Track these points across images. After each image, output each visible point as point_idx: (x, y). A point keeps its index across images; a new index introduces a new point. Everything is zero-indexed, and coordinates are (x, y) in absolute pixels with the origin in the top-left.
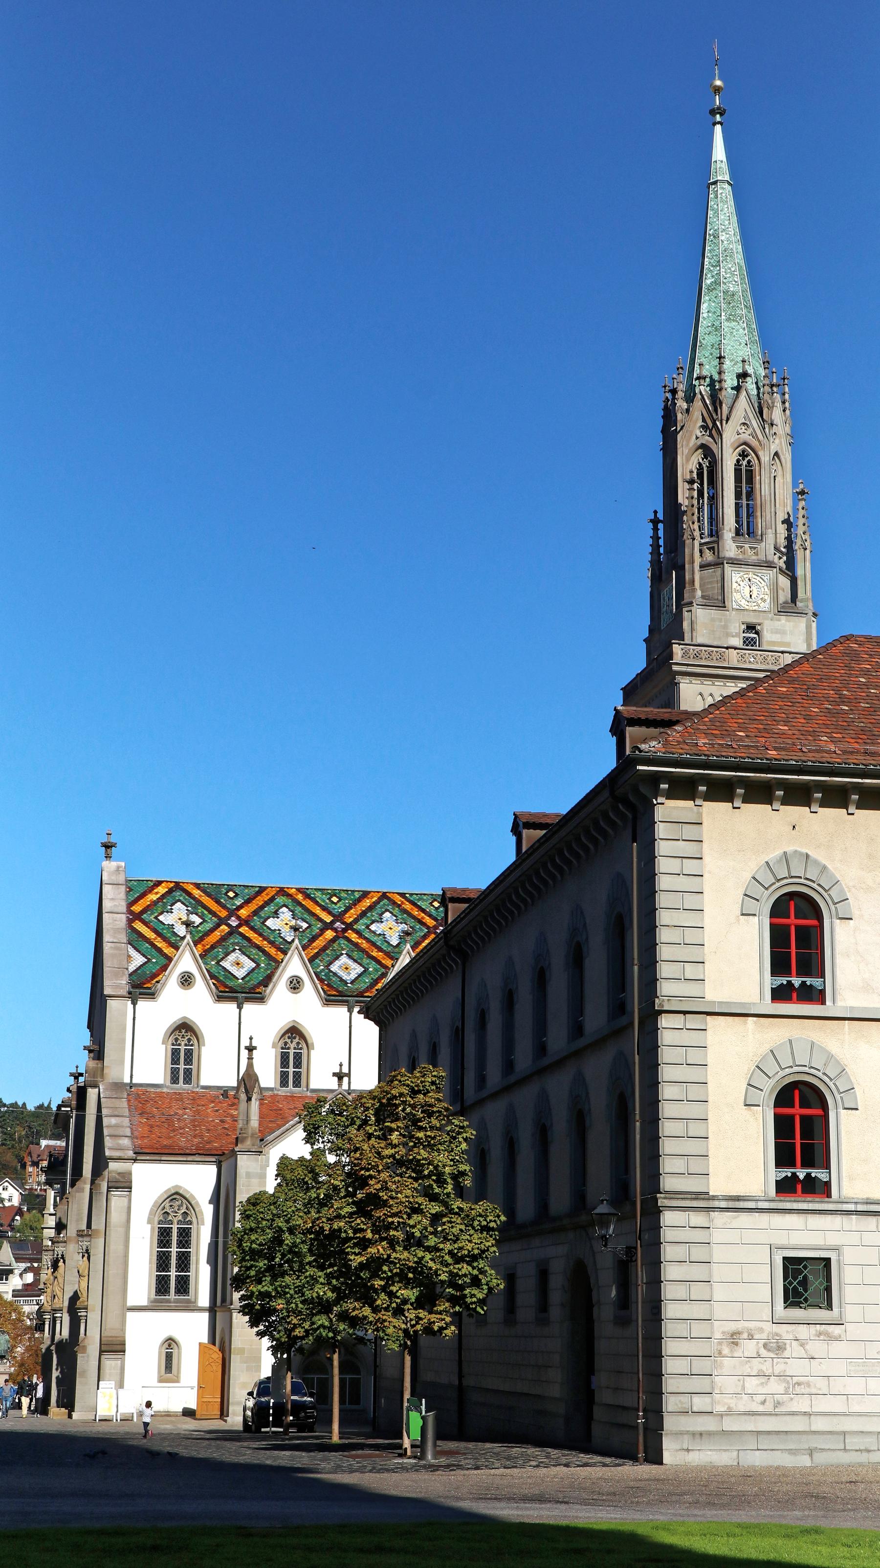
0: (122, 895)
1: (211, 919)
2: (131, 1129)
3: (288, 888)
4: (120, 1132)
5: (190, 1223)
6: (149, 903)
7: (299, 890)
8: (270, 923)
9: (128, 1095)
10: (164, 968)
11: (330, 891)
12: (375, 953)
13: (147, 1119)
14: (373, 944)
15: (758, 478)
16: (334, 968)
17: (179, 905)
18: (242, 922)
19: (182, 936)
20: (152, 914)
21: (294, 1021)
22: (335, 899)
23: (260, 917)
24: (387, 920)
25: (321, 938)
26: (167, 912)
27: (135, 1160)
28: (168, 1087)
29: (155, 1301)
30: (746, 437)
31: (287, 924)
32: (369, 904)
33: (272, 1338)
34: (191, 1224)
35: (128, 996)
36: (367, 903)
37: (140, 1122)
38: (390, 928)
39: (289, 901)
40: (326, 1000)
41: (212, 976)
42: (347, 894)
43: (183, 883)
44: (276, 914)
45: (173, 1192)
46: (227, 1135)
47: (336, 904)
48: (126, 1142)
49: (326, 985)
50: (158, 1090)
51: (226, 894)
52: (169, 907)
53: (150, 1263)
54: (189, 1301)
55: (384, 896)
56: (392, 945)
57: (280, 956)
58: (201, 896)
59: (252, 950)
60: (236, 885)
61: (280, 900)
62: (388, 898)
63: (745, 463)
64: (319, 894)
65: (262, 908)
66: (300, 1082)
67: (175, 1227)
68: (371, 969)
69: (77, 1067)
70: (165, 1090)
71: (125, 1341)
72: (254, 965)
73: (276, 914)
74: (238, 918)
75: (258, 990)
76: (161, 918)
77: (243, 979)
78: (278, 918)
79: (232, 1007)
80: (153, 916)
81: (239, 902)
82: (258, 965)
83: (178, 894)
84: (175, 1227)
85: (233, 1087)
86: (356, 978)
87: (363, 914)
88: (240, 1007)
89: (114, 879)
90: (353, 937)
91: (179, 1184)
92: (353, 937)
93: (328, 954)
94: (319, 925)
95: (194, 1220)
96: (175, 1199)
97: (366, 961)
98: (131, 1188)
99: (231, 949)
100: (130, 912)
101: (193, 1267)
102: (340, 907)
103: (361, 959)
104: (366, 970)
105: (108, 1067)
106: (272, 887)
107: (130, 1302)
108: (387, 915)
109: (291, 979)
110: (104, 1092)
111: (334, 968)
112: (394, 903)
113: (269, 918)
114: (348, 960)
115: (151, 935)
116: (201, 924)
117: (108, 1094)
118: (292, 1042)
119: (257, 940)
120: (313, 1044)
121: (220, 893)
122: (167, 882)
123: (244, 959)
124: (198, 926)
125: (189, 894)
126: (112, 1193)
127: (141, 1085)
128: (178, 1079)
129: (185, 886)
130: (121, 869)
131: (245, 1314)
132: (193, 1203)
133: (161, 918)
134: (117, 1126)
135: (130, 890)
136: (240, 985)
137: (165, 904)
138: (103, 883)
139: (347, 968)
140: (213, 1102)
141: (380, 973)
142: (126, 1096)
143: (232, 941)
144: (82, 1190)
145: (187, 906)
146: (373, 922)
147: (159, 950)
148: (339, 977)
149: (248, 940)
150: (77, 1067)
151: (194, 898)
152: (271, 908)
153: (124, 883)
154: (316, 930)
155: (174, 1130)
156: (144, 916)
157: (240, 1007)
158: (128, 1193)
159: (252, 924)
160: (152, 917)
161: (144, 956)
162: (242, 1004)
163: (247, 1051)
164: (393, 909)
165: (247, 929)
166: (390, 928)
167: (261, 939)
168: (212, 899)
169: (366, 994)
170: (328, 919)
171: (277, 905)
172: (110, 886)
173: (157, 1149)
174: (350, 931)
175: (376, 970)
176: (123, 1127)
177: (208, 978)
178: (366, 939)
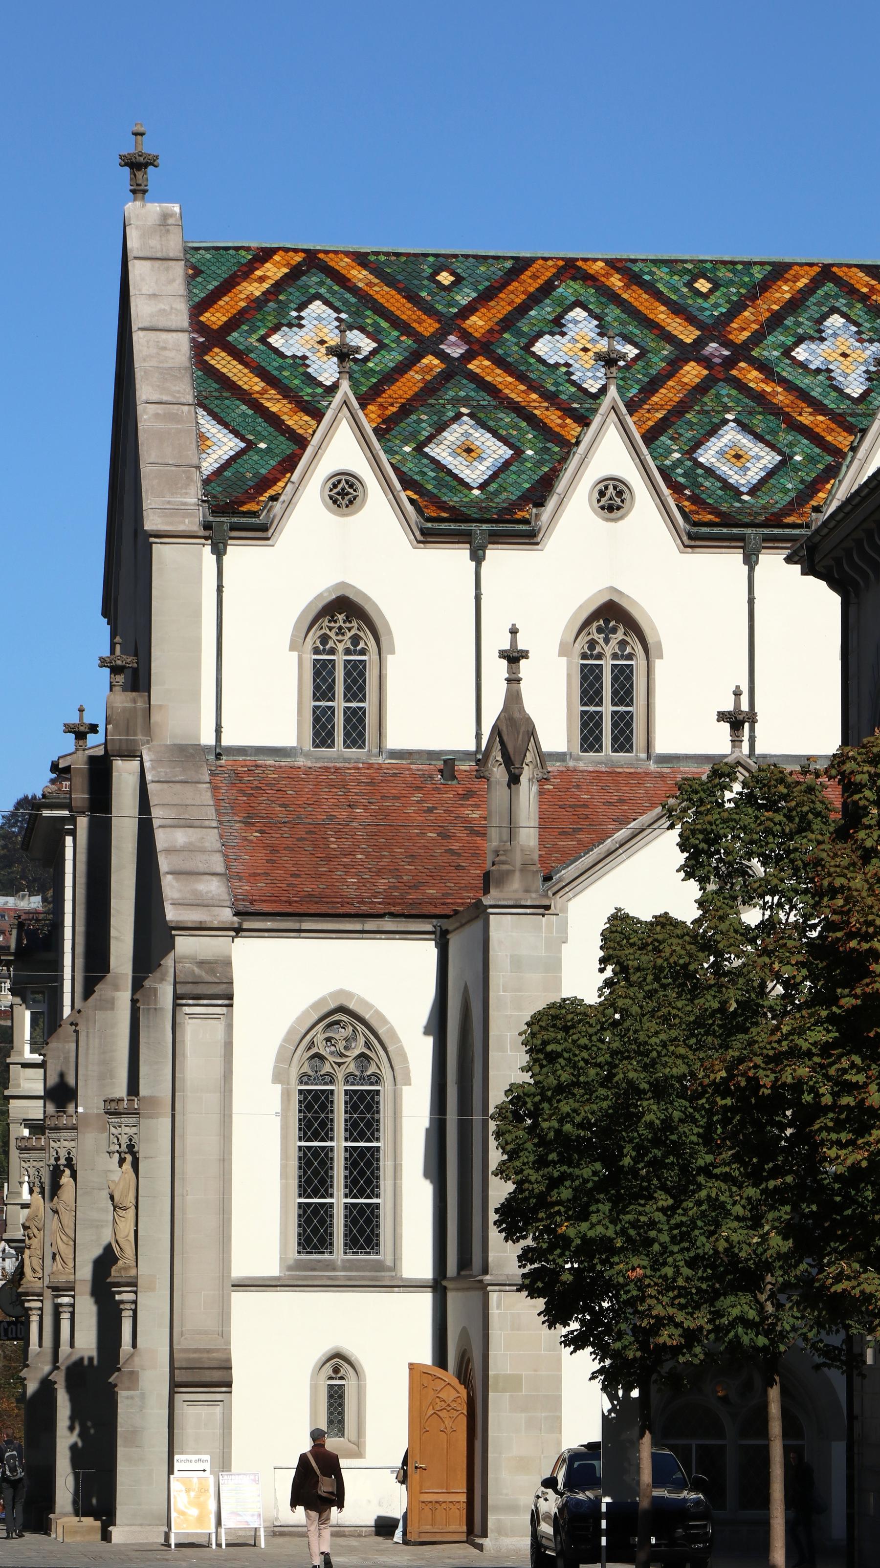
0: (178, 286)
1: (397, 340)
2: (226, 856)
3: (585, 260)
4: (199, 863)
5: (376, 1079)
6: (243, 304)
7: (613, 264)
8: (542, 347)
9: (213, 774)
10: (289, 464)
11: (689, 266)
12: (806, 419)
13: (262, 832)
14: (803, 395)
16: (707, 456)
17: (317, 307)
18: (476, 347)
19: (328, 383)
20: (252, 331)
21: (613, 589)
22: (703, 285)
23: (519, 334)
24: (835, 335)
25: (671, 383)
26: (290, 325)
27: (238, 931)
28: (307, 755)
29: (298, 1266)
31: (585, 350)
32: (788, 296)
33: (602, 1351)
34: (377, 1083)
35: (202, 533)
36: (785, 291)
37: (245, 839)
38: (844, 355)
39: (589, 294)
40: (690, 536)
41: (407, 483)
42: (734, 271)
43: (326, 252)
44: (557, 326)
45: (332, 1005)
46: (458, 867)
47: (705, 296)
48: (214, 888)
49: (689, 498)
50: (285, 762)
51: (432, 277)
52: (294, 314)
53: (284, 1175)
54: (379, 1266)
55: (826, 273)
56: (848, 397)
57: (572, 429)
58: (370, 284)
59: (501, 415)
60: (455, 256)
61: (567, 290)
62: (837, 281)
64: (662, 273)
65: (522, 310)
66: (629, 739)
67: (340, 1090)
68: (798, 458)
70: (301, 762)
71: (229, 1360)
72: (508, 453)
73: (557, 326)
74: (465, 336)
75: (520, 515)
76: (275, 340)
77: (482, 487)
78: (563, 334)
79: (460, 555)
80: (255, 337)
81: (464, 297)
82: (518, 453)
83: (312, 280)
84: (340, 1090)
85: (467, 754)
86: (763, 481)
87: (775, 321)
88: (478, 557)
89: (155, 245)
90: (753, 377)
91: (347, 988)
92: (753, 377)
93: (690, 424)
94: (666, 350)
95: (386, 1073)
96: (337, 1023)
97: (785, 438)
98: (230, 997)
99: (451, 414)
100: (198, 326)
101: (386, 1184)
102: (716, 306)
103: (774, 432)
104: (786, 460)
105: (160, 707)
106: (545, 259)
107: (239, 1270)
108: (836, 321)
109: (601, 486)
110: (153, 768)
111: (707, 456)
112: (851, 291)
113: (540, 335)
114: (739, 437)
115: (253, 384)
116: (374, 353)
117: (164, 772)
118: (607, 641)
119: (515, 390)
120: (659, 644)
121: (418, 275)
122: (287, 250)
123: (483, 439)
124: (366, 359)
125: (342, 280)
126: (187, 1010)
127: (242, 751)
128: (331, 734)
129: (332, 261)
130: (171, 221)
131: (533, 1293)
132: (381, 1032)
133: (275, 340)
134: (190, 850)
135: (195, 273)
136: (475, 503)
137: (283, 308)
138: (130, 255)
139: (738, 457)
140: (419, 788)
141: (821, 466)
142: (207, 778)
143: (451, 393)
144: (110, 1005)
145: (337, 310)
146: (800, 340)
147: (274, 420)
148: (719, 478)
149: (492, 390)
150: (81, 710)
151: (354, 290)
152: (546, 311)
153: (182, 255)
154: (659, 364)
155: (328, 859)
156: (234, 337)
157: (478, 557)
158: (224, 1010)
159: (500, 352)
160: (253, 340)
161: (236, 434)
162: (483, 548)
163: (504, 663)
164: (850, 306)
165: (487, 363)
166: (844, 355)
167: (523, 388)
168: (399, 291)
169: (790, 520)
170: (688, 335)
171: (560, 302)
172: (147, 264)
173: (290, 903)
174: (742, 364)
175: (810, 459)
176: (203, 851)
177: (398, 486)
178: (783, 382)
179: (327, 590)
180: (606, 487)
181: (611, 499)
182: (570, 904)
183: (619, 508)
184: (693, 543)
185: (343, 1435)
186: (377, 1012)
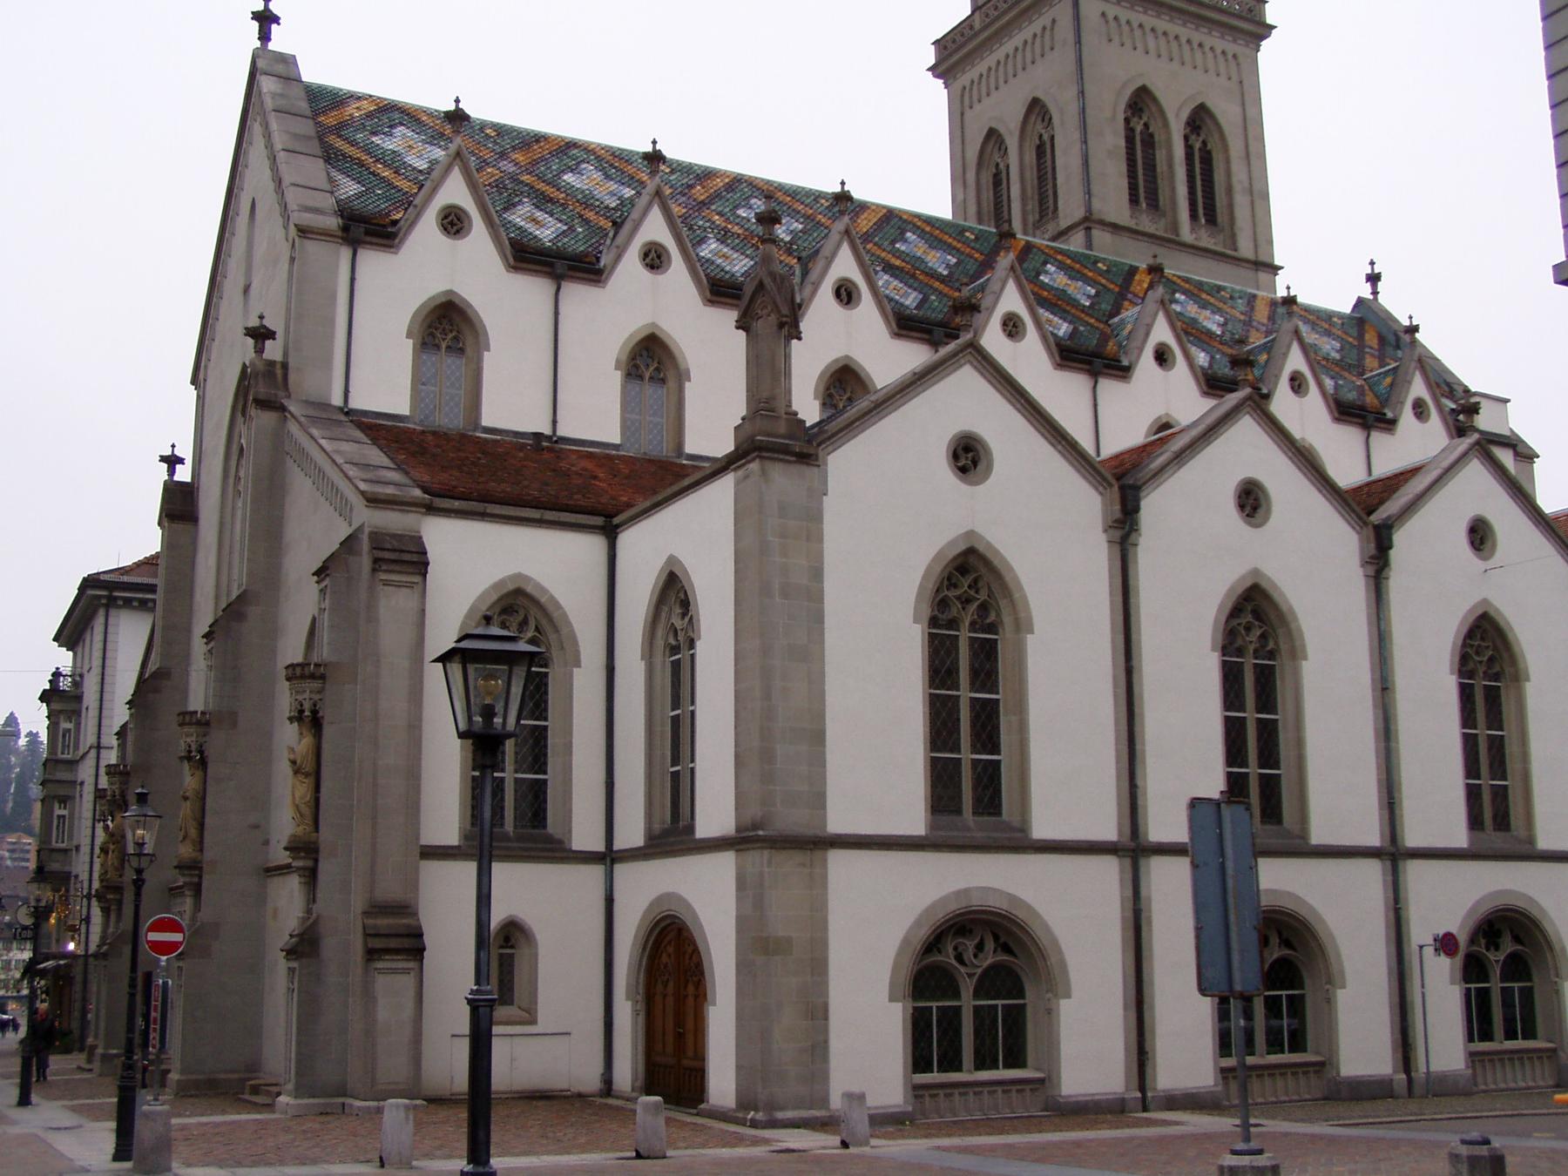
27: (431, 510)
35: (340, 233)
54: (550, 839)
69: (173, 446)
71: (421, 927)
85: (549, 438)
120: (688, 372)
127: (365, 413)
133: (376, 139)
150: (173, 446)
180: (650, 251)
181: (653, 259)
182: (829, 457)
184: (714, 298)
185: (511, 1003)
186: (552, 598)
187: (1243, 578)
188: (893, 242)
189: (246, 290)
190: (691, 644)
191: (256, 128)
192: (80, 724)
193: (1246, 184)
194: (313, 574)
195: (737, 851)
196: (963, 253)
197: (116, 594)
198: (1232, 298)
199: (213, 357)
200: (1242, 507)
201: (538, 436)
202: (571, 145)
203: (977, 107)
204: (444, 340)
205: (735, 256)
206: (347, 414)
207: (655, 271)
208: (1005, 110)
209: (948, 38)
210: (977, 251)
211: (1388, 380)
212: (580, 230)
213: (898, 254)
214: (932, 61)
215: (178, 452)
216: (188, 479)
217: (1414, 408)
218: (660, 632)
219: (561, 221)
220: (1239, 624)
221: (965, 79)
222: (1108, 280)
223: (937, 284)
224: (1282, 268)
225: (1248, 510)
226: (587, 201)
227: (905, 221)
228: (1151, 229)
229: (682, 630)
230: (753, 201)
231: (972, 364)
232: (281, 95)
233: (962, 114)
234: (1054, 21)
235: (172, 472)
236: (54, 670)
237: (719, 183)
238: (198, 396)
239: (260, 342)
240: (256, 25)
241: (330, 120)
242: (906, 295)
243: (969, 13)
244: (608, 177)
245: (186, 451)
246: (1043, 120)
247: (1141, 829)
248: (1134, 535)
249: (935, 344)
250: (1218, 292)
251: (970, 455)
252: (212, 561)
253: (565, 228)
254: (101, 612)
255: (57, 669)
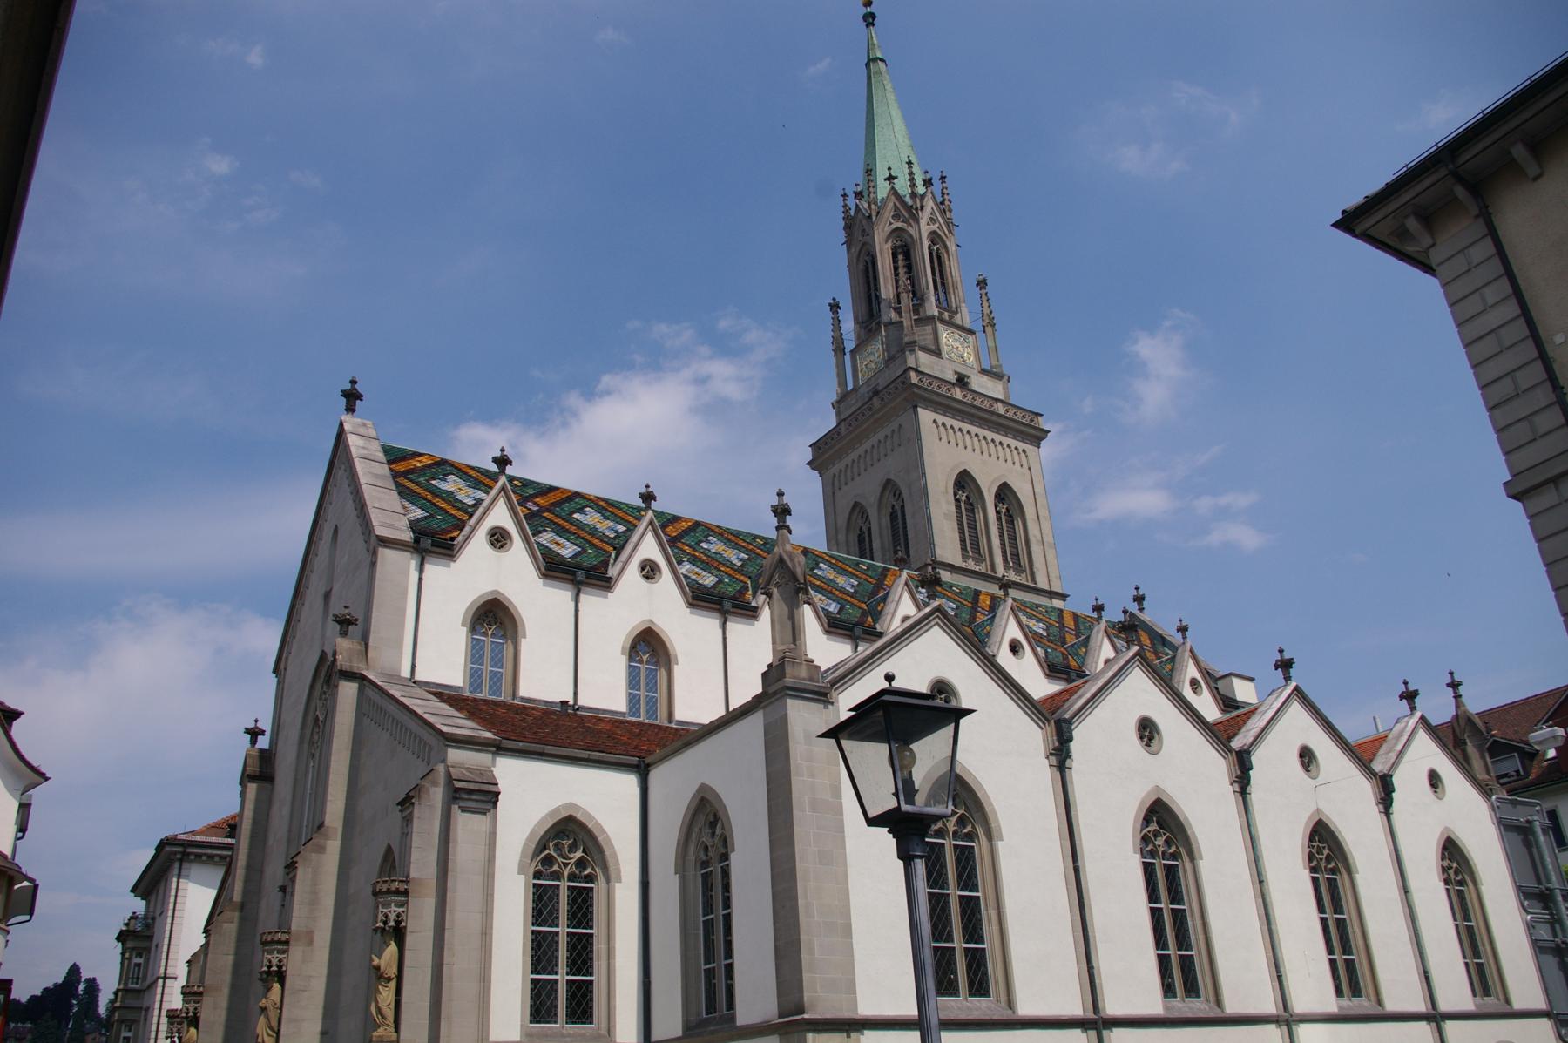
15: (947, 263)
27: (499, 749)
30: (934, 227)
63: (935, 248)
84: (564, 885)
101: (599, 964)
120: (676, 656)
144: (321, 849)
150: (256, 721)
179: (486, 593)
180: (646, 566)
181: (648, 572)
183: (652, 579)
184: (695, 602)
187: (1149, 794)
188: (813, 569)
189: (327, 596)
190: (725, 857)
191: (340, 473)
192: (148, 959)
193: (1039, 538)
194: (398, 804)
195: (780, 1035)
196: (861, 578)
197: (189, 850)
198: (1047, 612)
199: (293, 651)
200: (1141, 738)
201: (564, 703)
202: (577, 494)
203: (845, 488)
204: (490, 629)
205: (704, 573)
206: (414, 683)
207: (650, 580)
208: (867, 488)
209: (822, 441)
210: (871, 577)
211: (1169, 667)
212: (590, 551)
213: (817, 577)
214: (810, 458)
215: (260, 725)
216: (267, 748)
217: (1191, 685)
218: (692, 847)
219: (576, 545)
220: (1149, 832)
221: (834, 469)
222: (962, 598)
223: (848, 598)
224: (1069, 596)
225: (1145, 739)
226: (593, 531)
227: (817, 556)
228: (977, 569)
229: (713, 847)
230: (710, 538)
231: (939, 626)
232: (363, 448)
233: (834, 493)
234: (900, 426)
235: (254, 742)
236: (131, 914)
237: (684, 525)
238: (279, 683)
239: (345, 626)
240: (344, 400)
241: (401, 467)
242: (830, 605)
243: (835, 424)
244: (605, 518)
245: (266, 724)
246: (894, 495)
247: (1100, 1005)
248: (1068, 761)
249: (855, 640)
250: (1037, 608)
251: (943, 696)
252: (286, 811)
253: (580, 549)
254: (177, 865)
255: (134, 913)
